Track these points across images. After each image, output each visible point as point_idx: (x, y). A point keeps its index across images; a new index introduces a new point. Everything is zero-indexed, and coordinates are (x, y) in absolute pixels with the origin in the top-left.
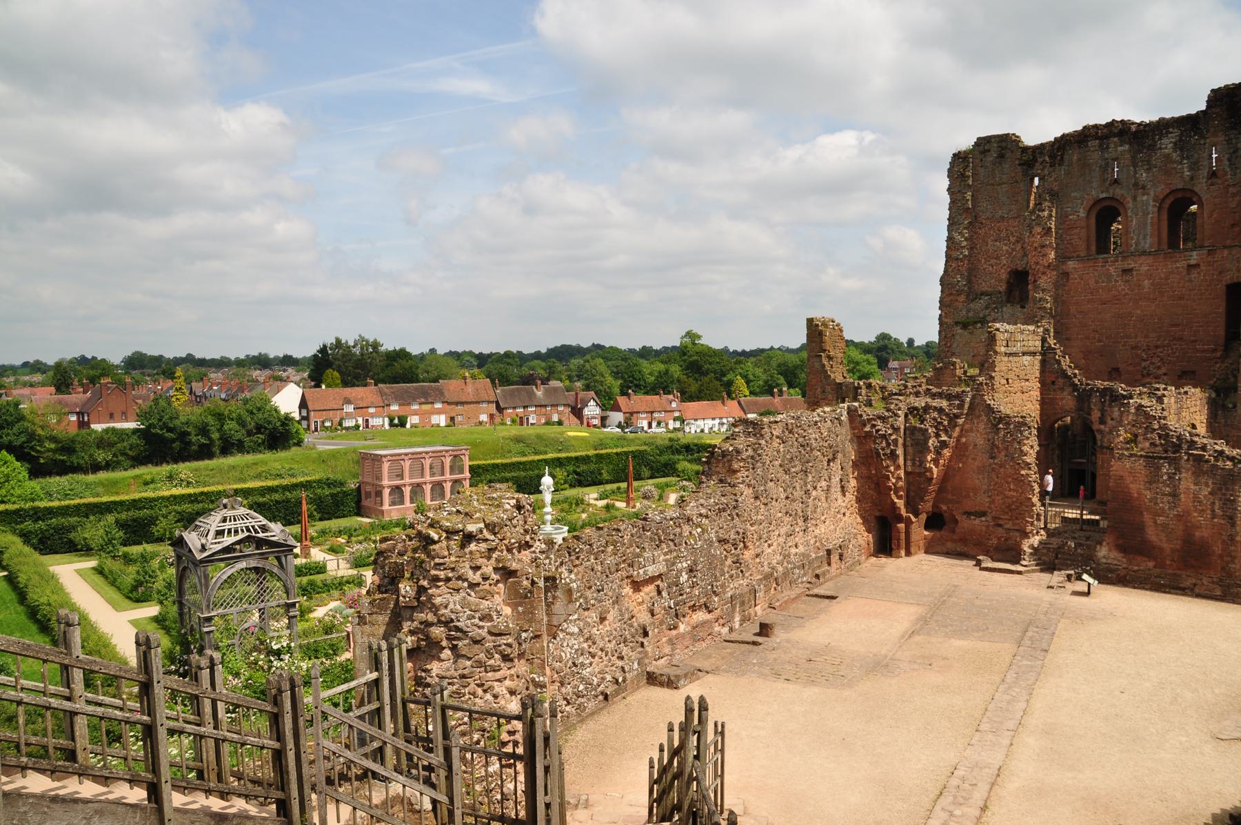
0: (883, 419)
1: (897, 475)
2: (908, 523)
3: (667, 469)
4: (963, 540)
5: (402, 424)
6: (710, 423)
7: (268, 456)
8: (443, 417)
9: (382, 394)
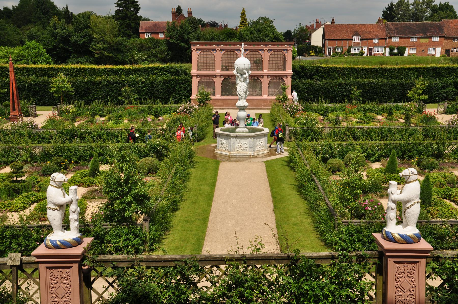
5: (401, 52)
8: (439, 50)
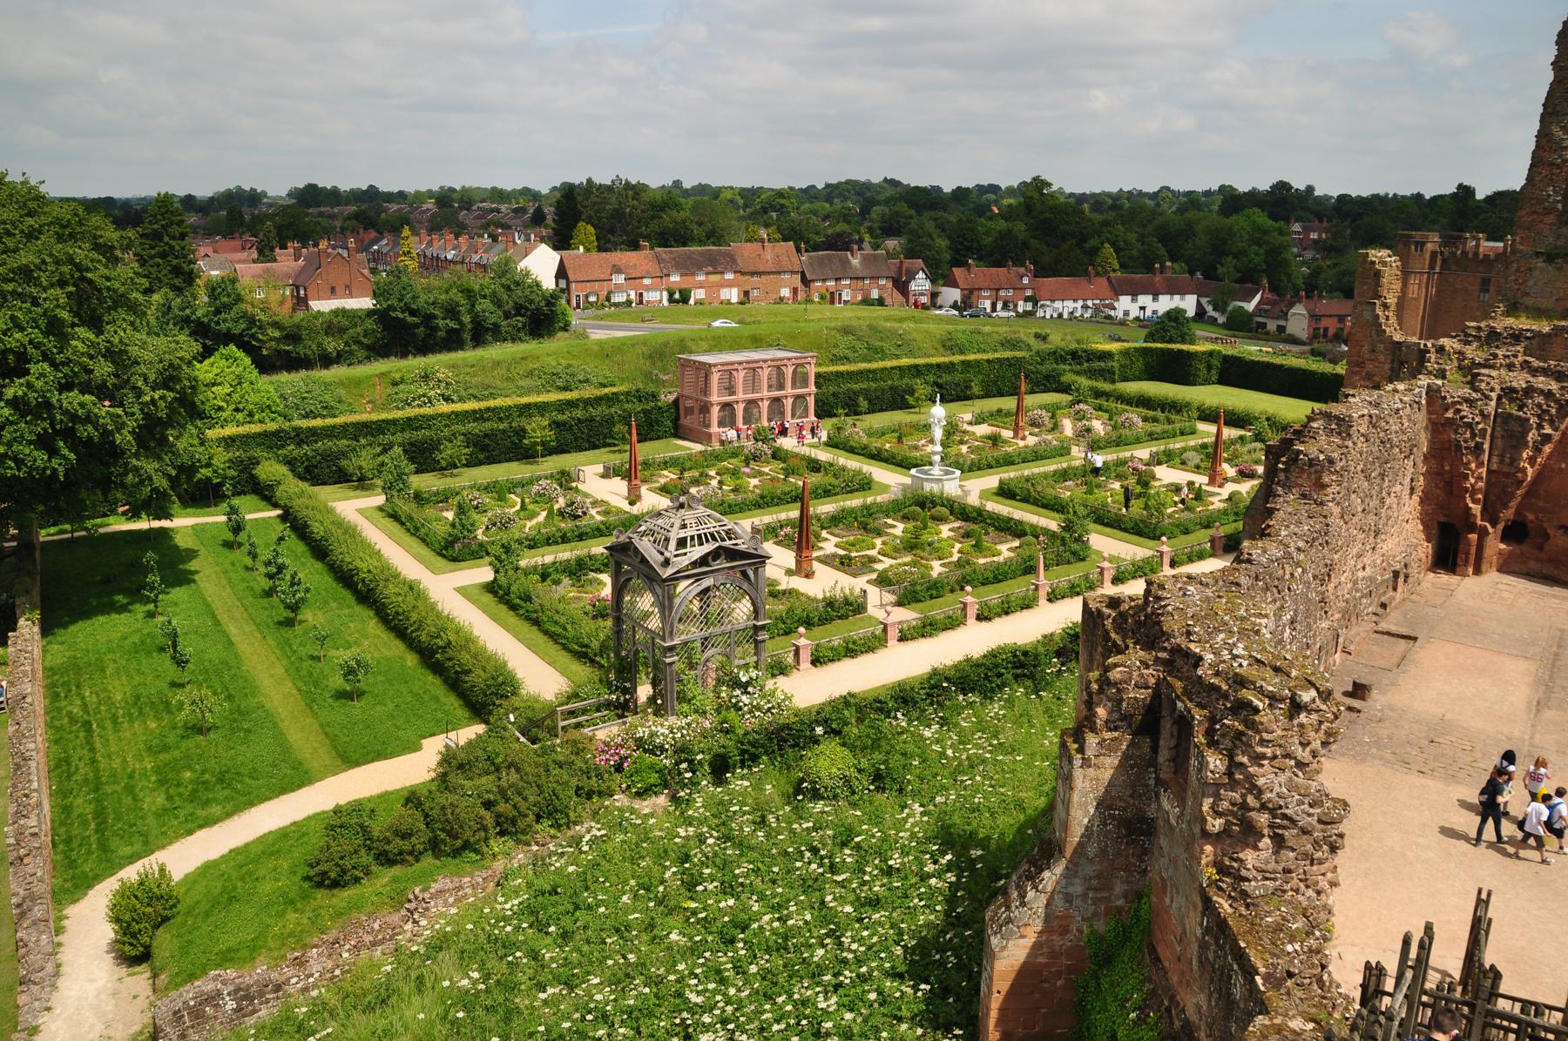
0: (1470, 402)
1: (1477, 475)
2: (1483, 533)
3: (1050, 383)
4: (1554, 561)
5: (685, 299)
6: (1070, 305)
7: (530, 347)
8: (735, 291)
9: (659, 260)
